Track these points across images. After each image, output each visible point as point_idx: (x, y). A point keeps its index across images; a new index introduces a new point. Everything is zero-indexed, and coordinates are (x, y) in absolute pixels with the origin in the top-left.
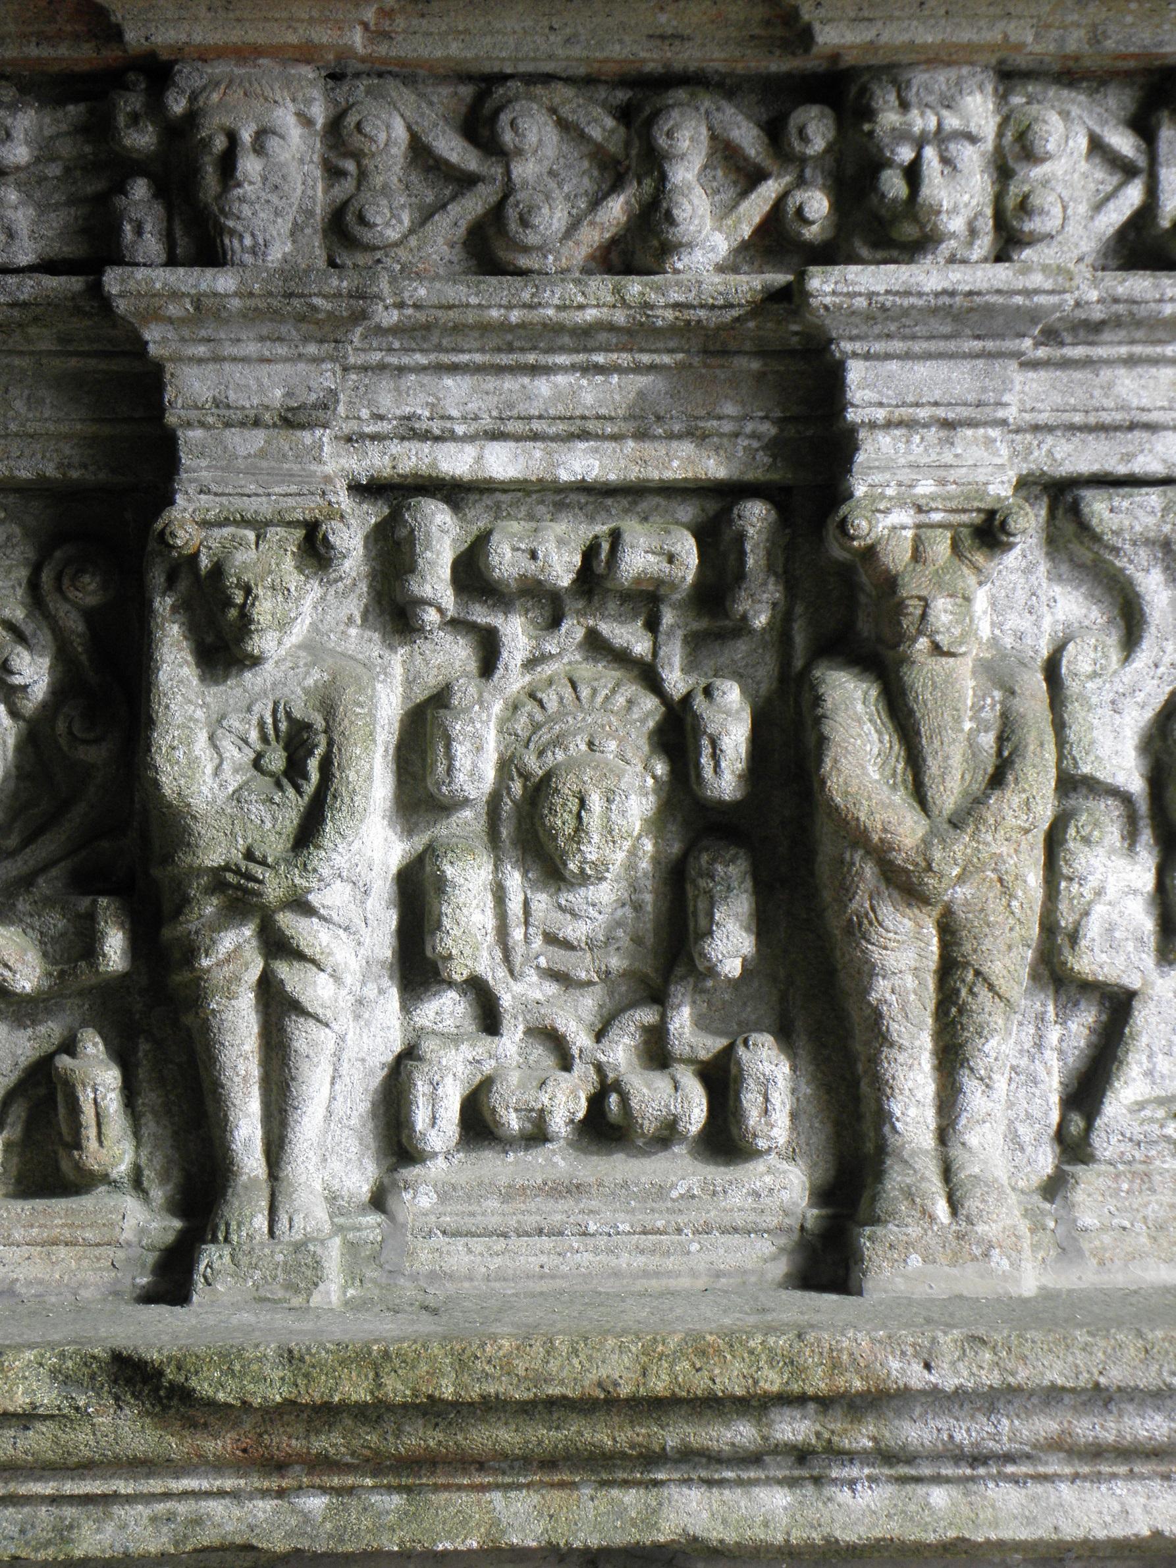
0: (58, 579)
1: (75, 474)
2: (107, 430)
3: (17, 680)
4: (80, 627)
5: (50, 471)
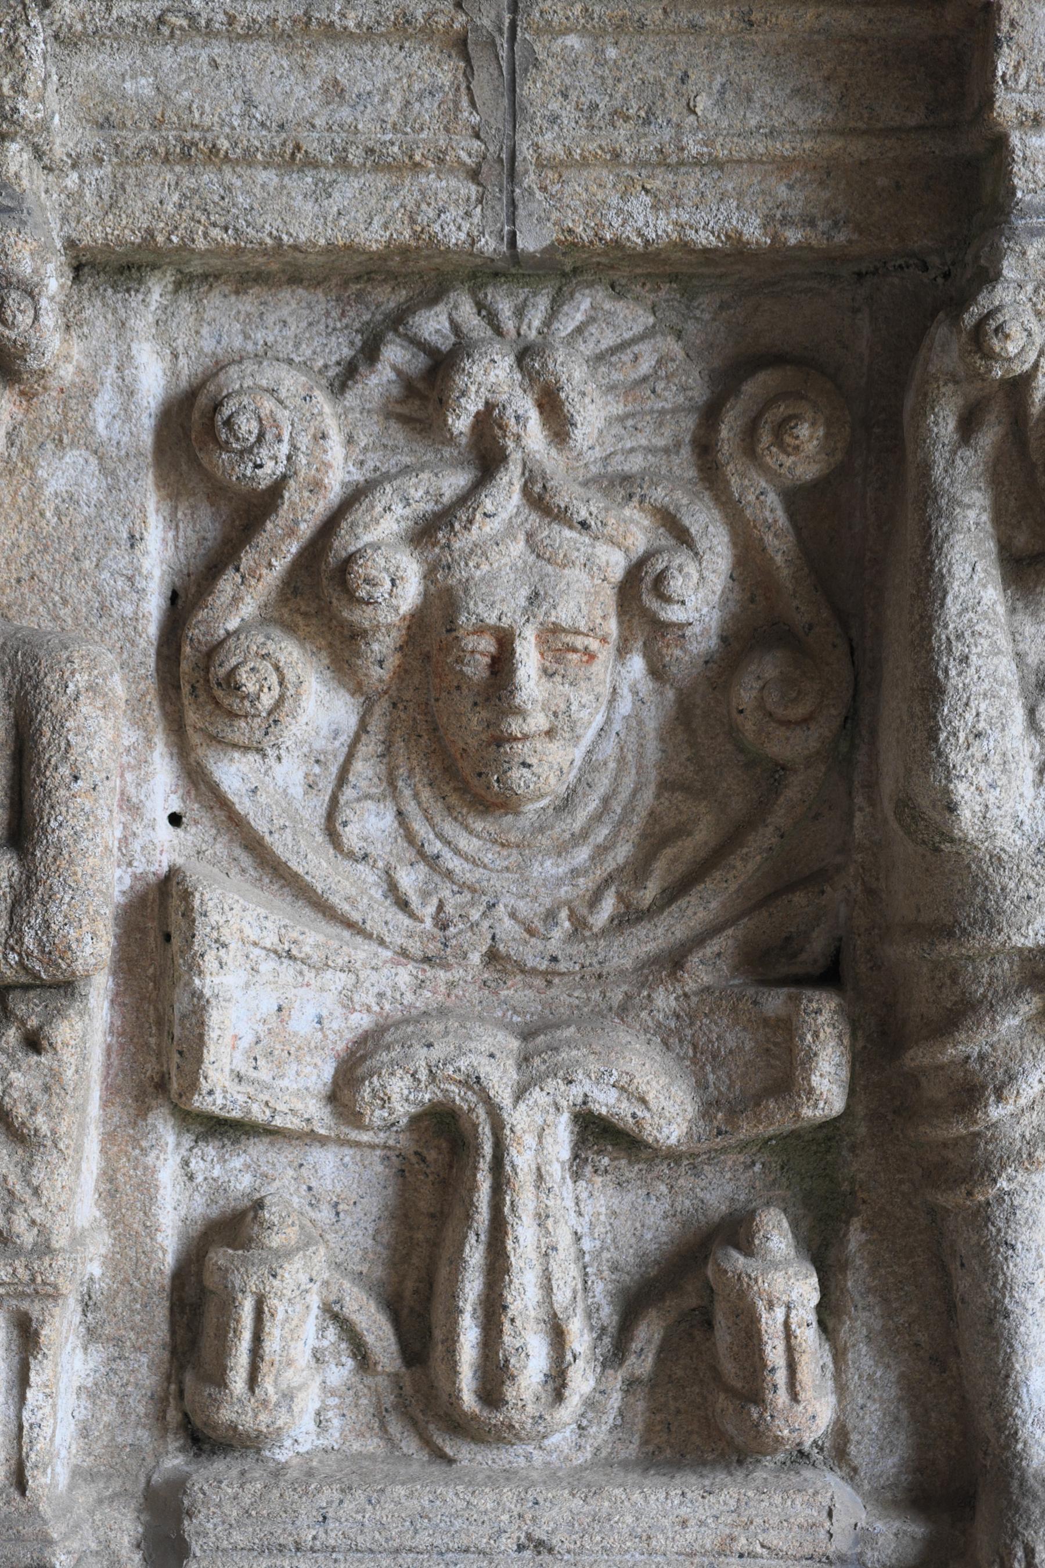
0: (750, 433)
1: (793, 236)
2: (858, 148)
3: (674, 614)
4: (781, 517)
5: (753, 232)
